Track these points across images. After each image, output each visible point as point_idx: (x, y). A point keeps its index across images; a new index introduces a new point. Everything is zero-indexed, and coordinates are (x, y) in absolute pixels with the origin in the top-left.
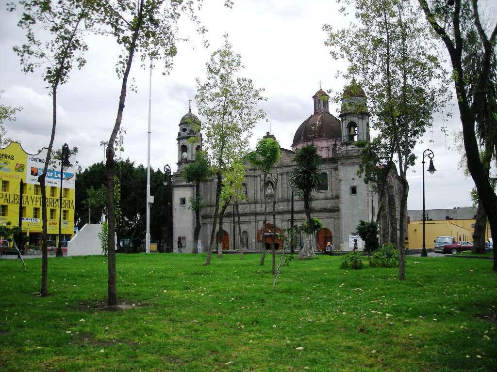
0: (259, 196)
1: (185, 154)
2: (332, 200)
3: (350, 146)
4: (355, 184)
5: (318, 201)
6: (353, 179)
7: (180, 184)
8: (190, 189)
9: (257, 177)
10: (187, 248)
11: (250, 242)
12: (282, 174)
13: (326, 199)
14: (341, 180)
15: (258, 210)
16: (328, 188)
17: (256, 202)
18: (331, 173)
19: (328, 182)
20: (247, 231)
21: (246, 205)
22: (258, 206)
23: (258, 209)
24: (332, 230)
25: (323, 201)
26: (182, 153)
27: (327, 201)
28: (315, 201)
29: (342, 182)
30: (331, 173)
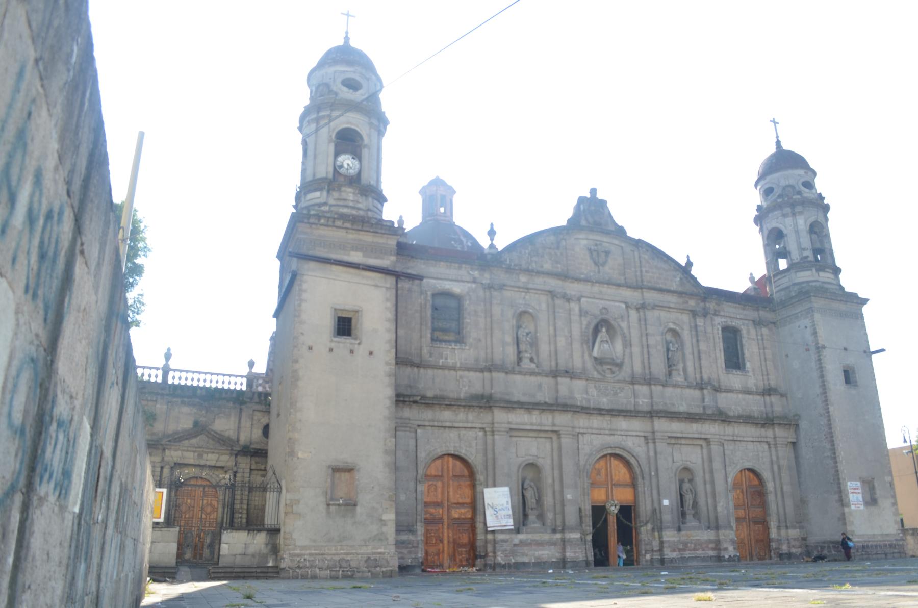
0: (578, 359)
1: (347, 162)
2: (758, 397)
3: (821, 274)
4: (851, 360)
5: (730, 395)
6: (845, 349)
7: (334, 256)
8: (391, 280)
9: (568, 300)
10: (358, 509)
11: (548, 500)
12: (641, 307)
13: (748, 392)
14: (824, 347)
15: (579, 398)
16: (748, 365)
17: (570, 374)
18: (748, 332)
19: (746, 352)
20: (540, 462)
21: (539, 379)
22: (579, 384)
23: (578, 396)
24: (766, 475)
25: (740, 396)
26: (337, 154)
27: (747, 396)
28: (724, 395)
29: (826, 353)
30: (748, 332)
